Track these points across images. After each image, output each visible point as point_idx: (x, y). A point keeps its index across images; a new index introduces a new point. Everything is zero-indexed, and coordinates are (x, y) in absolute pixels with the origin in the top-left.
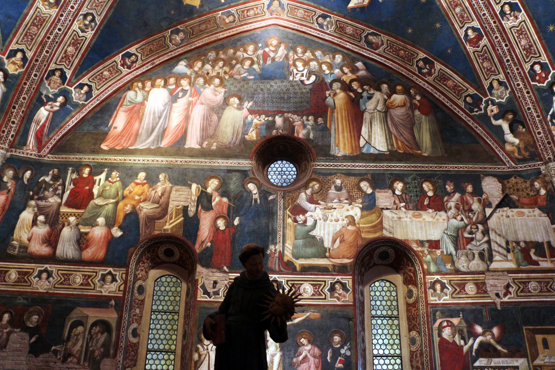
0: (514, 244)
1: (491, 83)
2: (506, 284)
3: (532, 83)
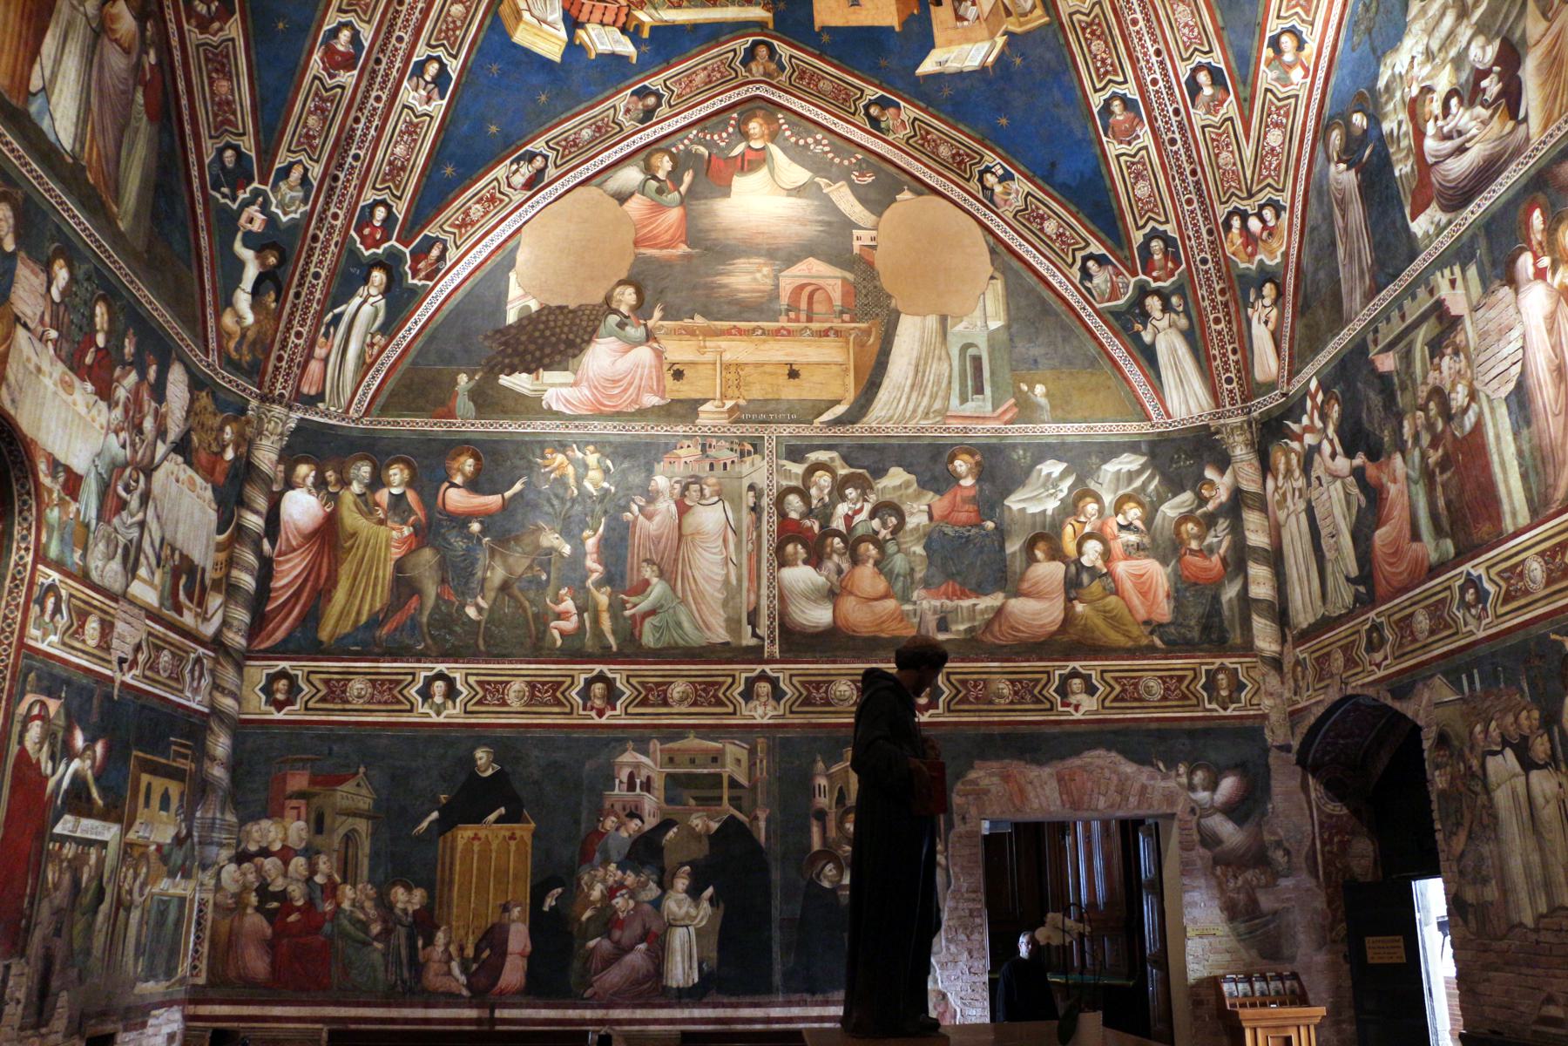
0: (169, 552)
1: (291, 165)
2: (137, 640)
3: (352, 232)
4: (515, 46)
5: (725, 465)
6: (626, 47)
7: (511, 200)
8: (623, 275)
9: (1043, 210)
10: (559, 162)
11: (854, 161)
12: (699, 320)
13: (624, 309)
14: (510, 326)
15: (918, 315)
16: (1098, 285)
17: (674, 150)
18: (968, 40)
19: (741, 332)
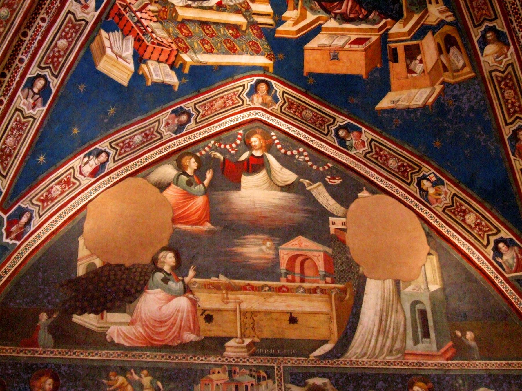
4: (97, 71)
5: (246, 386)
6: (172, 79)
7: (80, 184)
8: (165, 243)
9: (465, 206)
10: (116, 159)
11: (327, 168)
12: (223, 279)
13: (166, 268)
14: (80, 278)
15: (378, 279)
16: (507, 260)
17: (198, 154)
18: (415, 87)
19: (253, 288)
